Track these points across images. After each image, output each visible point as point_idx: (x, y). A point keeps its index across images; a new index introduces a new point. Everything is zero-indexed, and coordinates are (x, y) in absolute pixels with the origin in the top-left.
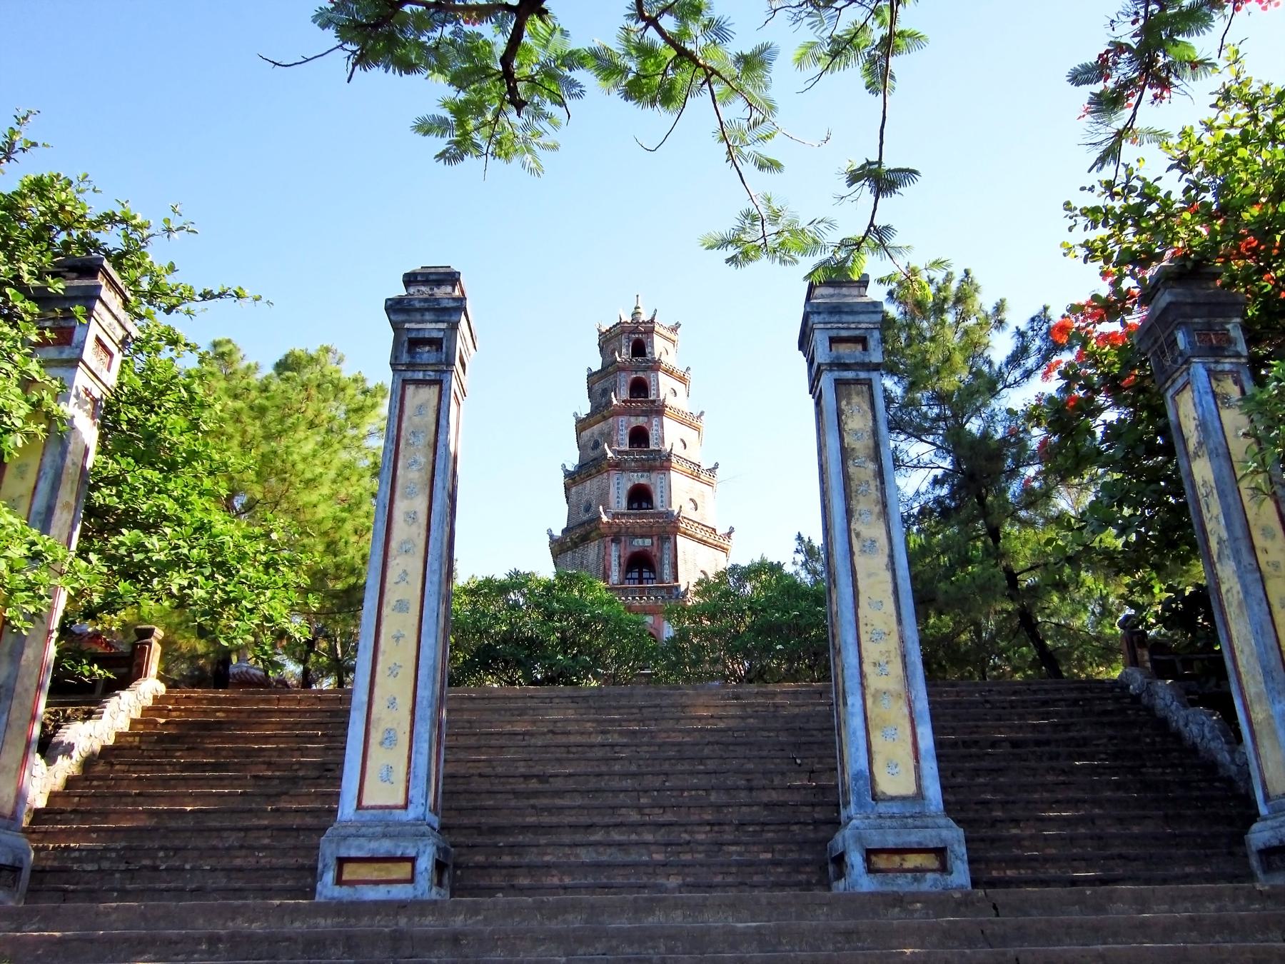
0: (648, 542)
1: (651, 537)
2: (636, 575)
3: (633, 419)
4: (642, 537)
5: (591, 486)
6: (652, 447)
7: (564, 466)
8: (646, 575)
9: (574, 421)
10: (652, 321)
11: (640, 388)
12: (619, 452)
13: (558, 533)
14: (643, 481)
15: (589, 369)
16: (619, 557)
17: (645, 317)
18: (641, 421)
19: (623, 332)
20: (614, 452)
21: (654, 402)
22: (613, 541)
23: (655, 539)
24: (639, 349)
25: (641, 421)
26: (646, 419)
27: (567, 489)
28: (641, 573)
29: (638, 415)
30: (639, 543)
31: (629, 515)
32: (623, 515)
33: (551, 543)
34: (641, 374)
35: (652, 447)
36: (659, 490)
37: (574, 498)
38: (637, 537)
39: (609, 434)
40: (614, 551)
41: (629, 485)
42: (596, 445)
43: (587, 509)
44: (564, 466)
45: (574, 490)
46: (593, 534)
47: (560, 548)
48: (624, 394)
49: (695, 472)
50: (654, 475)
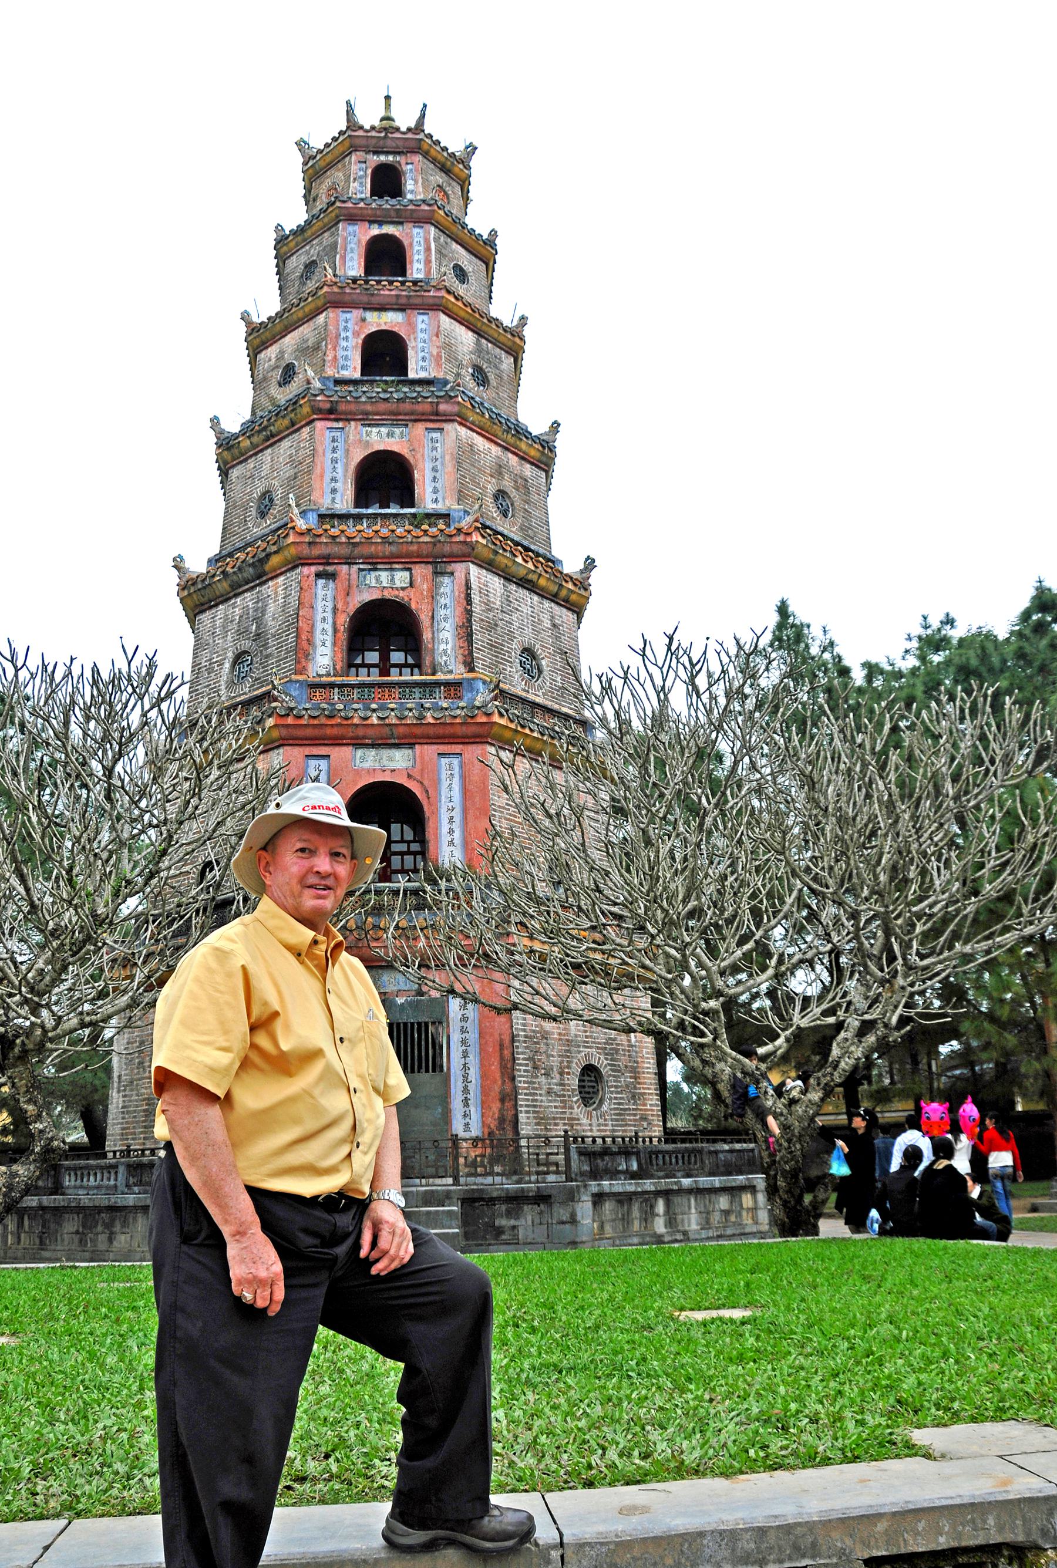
0: (401, 578)
3: (372, 317)
5: (273, 465)
6: (412, 375)
7: (215, 422)
9: (242, 329)
11: (386, 257)
12: (338, 382)
13: (198, 565)
15: (279, 228)
17: (405, 120)
18: (390, 320)
19: (354, 148)
20: (323, 380)
21: (415, 283)
22: (318, 575)
24: (387, 181)
25: (390, 320)
27: (224, 472)
28: (385, 657)
29: (382, 308)
31: (358, 518)
32: (343, 517)
33: (182, 587)
34: (389, 229)
35: (412, 375)
37: (236, 487)
39: (317, 348)
40: (324, 594)
41: (358, 455)
42: (289, 373)
43: (263, 514)
44: (215, 422)
45: (235, 473)
46: (275, 560)
47: (199, 597)
48: (355, 267)
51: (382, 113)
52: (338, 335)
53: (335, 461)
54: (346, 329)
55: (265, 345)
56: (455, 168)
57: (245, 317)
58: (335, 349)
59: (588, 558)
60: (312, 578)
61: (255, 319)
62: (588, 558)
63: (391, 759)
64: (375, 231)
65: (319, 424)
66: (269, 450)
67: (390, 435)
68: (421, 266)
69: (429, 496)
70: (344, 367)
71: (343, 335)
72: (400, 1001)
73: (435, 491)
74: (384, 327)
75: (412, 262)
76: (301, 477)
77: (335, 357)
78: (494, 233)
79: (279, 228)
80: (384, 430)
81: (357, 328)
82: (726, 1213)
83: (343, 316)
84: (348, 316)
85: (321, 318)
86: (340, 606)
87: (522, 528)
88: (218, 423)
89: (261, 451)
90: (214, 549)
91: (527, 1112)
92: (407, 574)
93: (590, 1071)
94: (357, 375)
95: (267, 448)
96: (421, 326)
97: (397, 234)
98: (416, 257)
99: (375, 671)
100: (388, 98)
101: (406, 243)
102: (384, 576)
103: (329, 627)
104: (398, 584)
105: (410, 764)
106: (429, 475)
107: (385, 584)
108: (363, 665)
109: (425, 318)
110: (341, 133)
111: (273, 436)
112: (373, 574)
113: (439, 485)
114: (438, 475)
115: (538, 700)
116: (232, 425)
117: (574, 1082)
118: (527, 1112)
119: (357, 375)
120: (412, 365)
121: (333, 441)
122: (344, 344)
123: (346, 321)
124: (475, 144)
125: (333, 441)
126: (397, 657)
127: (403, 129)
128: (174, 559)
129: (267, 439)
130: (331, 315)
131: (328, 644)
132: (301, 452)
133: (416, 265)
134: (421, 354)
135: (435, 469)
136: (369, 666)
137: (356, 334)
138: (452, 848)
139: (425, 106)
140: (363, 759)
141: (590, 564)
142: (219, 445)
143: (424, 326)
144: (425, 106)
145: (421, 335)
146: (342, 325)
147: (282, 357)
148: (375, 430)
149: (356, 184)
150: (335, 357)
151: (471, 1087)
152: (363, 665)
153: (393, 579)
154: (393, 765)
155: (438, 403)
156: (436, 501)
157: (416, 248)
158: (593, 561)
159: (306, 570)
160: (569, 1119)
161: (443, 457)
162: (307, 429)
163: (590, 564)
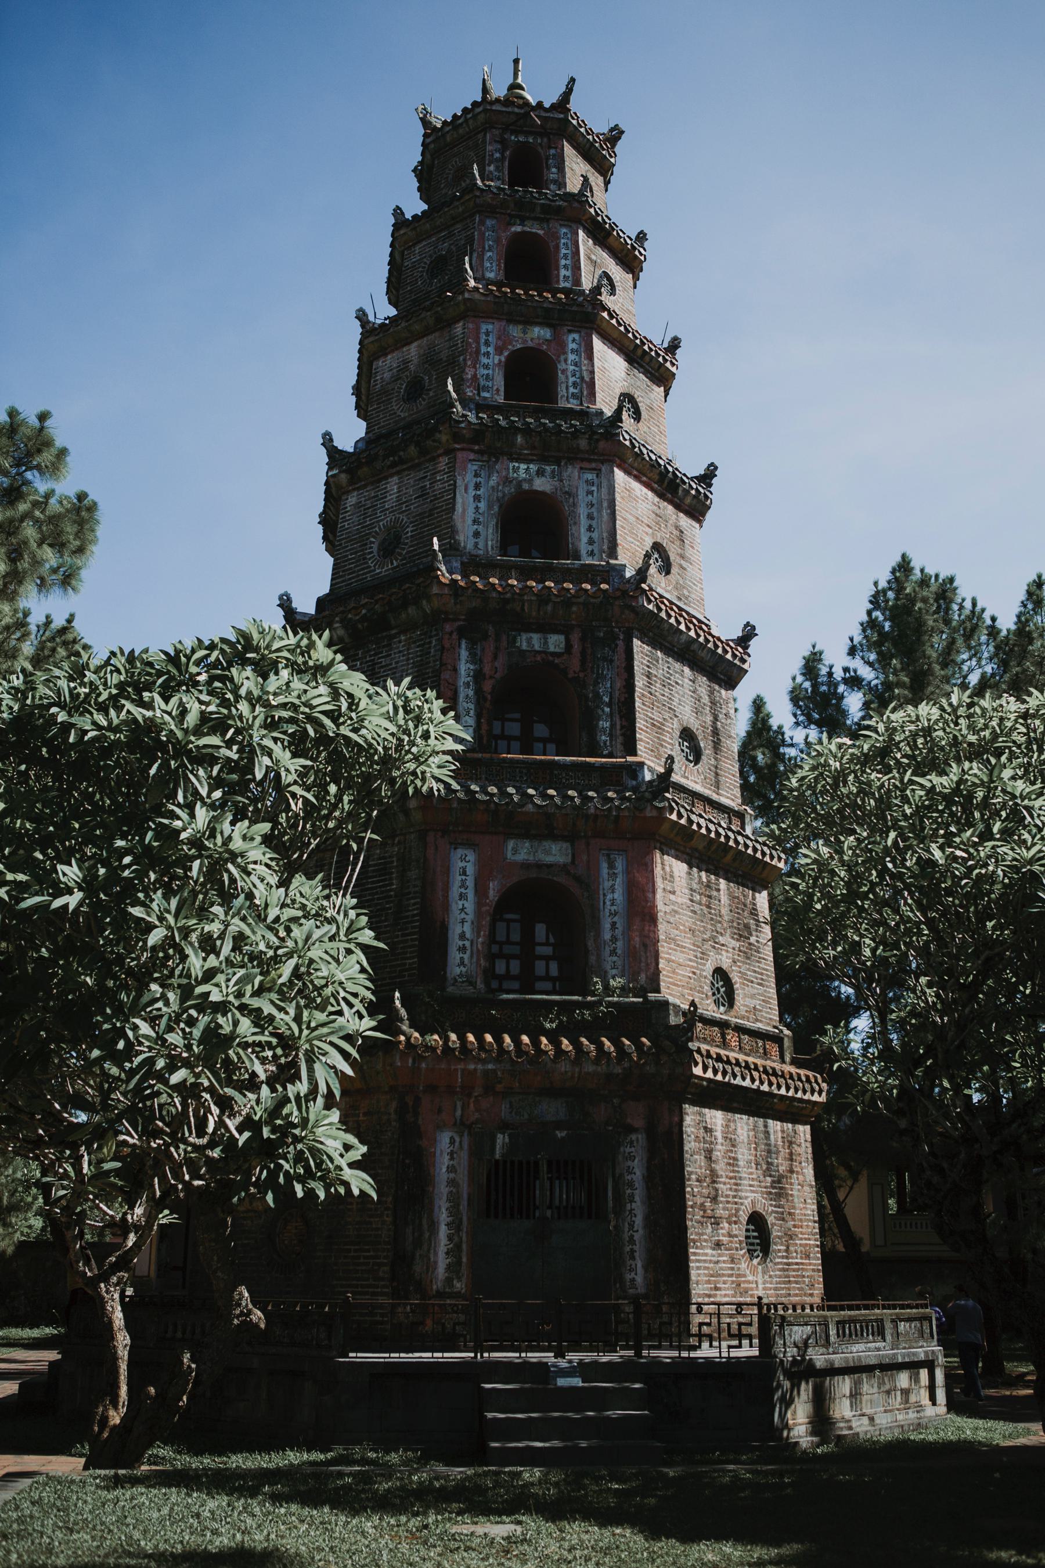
0: (555, 642)
1: (565, 630)
2: (514, 729)
3: (515, 331)
4: (544, 628)
7: (327, 440)
8: (541, 730)
9: (356, 330)
10: (563, 104)
14: (541, 484)
15: (398, 212)
16: (478, 677)
22: (462, 633)
23: (575, 637)
26: (546, 333)
30: (530, 641)
31: (504, 570)
35: (562, 404)
36: (583, 511)
38: (529, 629)
44: (327, 440)
49: (666, 484)
50: (572, 472)
51: (510, 80)
52: (478, 351)
53: (477, 498)
54: (487, 344)
55: (383, 352)
56: (599, 155)
57: (361, 316)
58: (475, 367)
59: (748, 624)
60: (455, 636)
61: (371, 318)
62: (748, 624)
63: (548, 852)
64: (519, 229)
65: (459, 455)
66: (395, 479)
67: (540, 473)
68: (568, 273)
69: (584, 548)
70: (486, 389)
71: (483, 349)
72: (560, 1134)
73: (591, 542)
74: (530, 344)
75: (558, 269)
76: (438, 515)
77: (475, 375)
78: (642, 237)
79: (398, 212)
80: (533, 467)
81: (500, 343)
82: (906, 1392)
83: (484, 328)
84: (490, 327)
85: (459, 328)
86: (487, 670)
87: (678, 587)
88: (331, 440)
89: (386, 478)
90: (325, 589)
91: (698, 1268)
92: (562, 638)
93: (756, 1220)
94: (501, 399)
95: (392, 475)
96: (572, 346)
97: (541, 232)
98: (563, 262)
99: (516, 745)
100: (516, 61)
101: (552, 244)
102: (536, 638)
103: (471, 693)
104: (552, 649)
105: (569, 859)
106: (584, 522)
107: (537, 648)
108: (503, 736)
109: (576, 336)
110: (475, 104)
111: (402, 461)
112: (524, 636)
113: (595, 535)
114: (594, 523)
115: (698, 788)
116: (346, 443)
117: (740, 1231)
118: (698, 1268)
119: (501, 399)
120: (562, 391)
121: (476, 475)
122: (484, 360)
123: (487, 334)
124: (622, 127)
125: (476, 475)
126: (541, 730)
127: (547, 105)
128: (281, 598)
129: (394, 465)
130: (471, 326)
131: (472, 713)
132: (438, 486)
133: (563, 272)
134: (572, 380)
135: (590, 517)
136: (510, 739)
137: (499, 350)
138: (615, 958)
139: (573, 80)
140: (515, 851)
141: (748, 634)
142: (331, 465)
143: (574, 346)
144: (573, 80)
145: (571, 357)
146: (483, 338)
147: (407, 368)
148: (523, 466)
149: (492, 168)
150: (475, 375)
151: (637, 1236)
152: (503, 736)
153: (546, 643)
154: (549, 859)
155: (598, 441)
156: (591, 554)
157: (563, 251)
158: (754, 628)
159: (448, 628)
160: (739, 1276)
161: (600, 503)
162: (444, 461)
163: (748, 634)
